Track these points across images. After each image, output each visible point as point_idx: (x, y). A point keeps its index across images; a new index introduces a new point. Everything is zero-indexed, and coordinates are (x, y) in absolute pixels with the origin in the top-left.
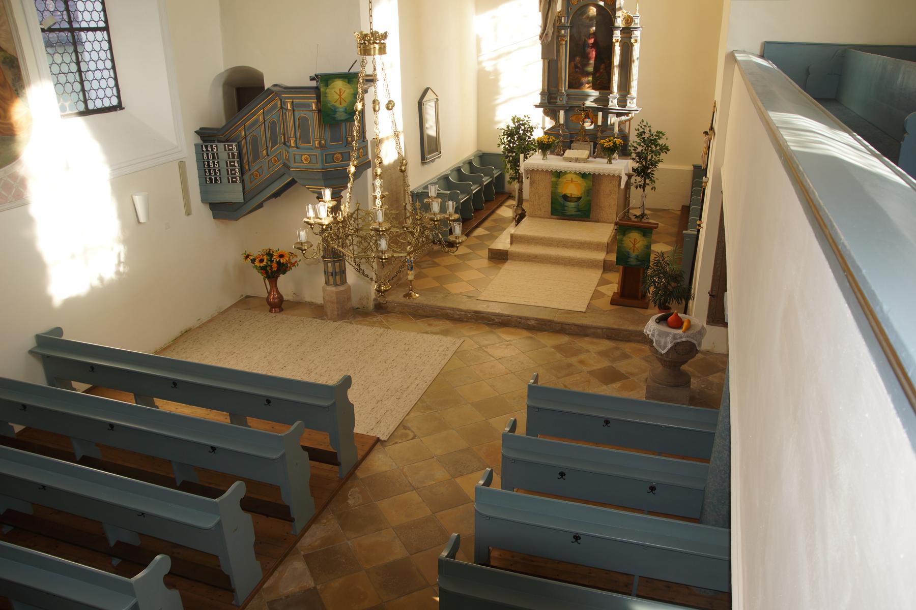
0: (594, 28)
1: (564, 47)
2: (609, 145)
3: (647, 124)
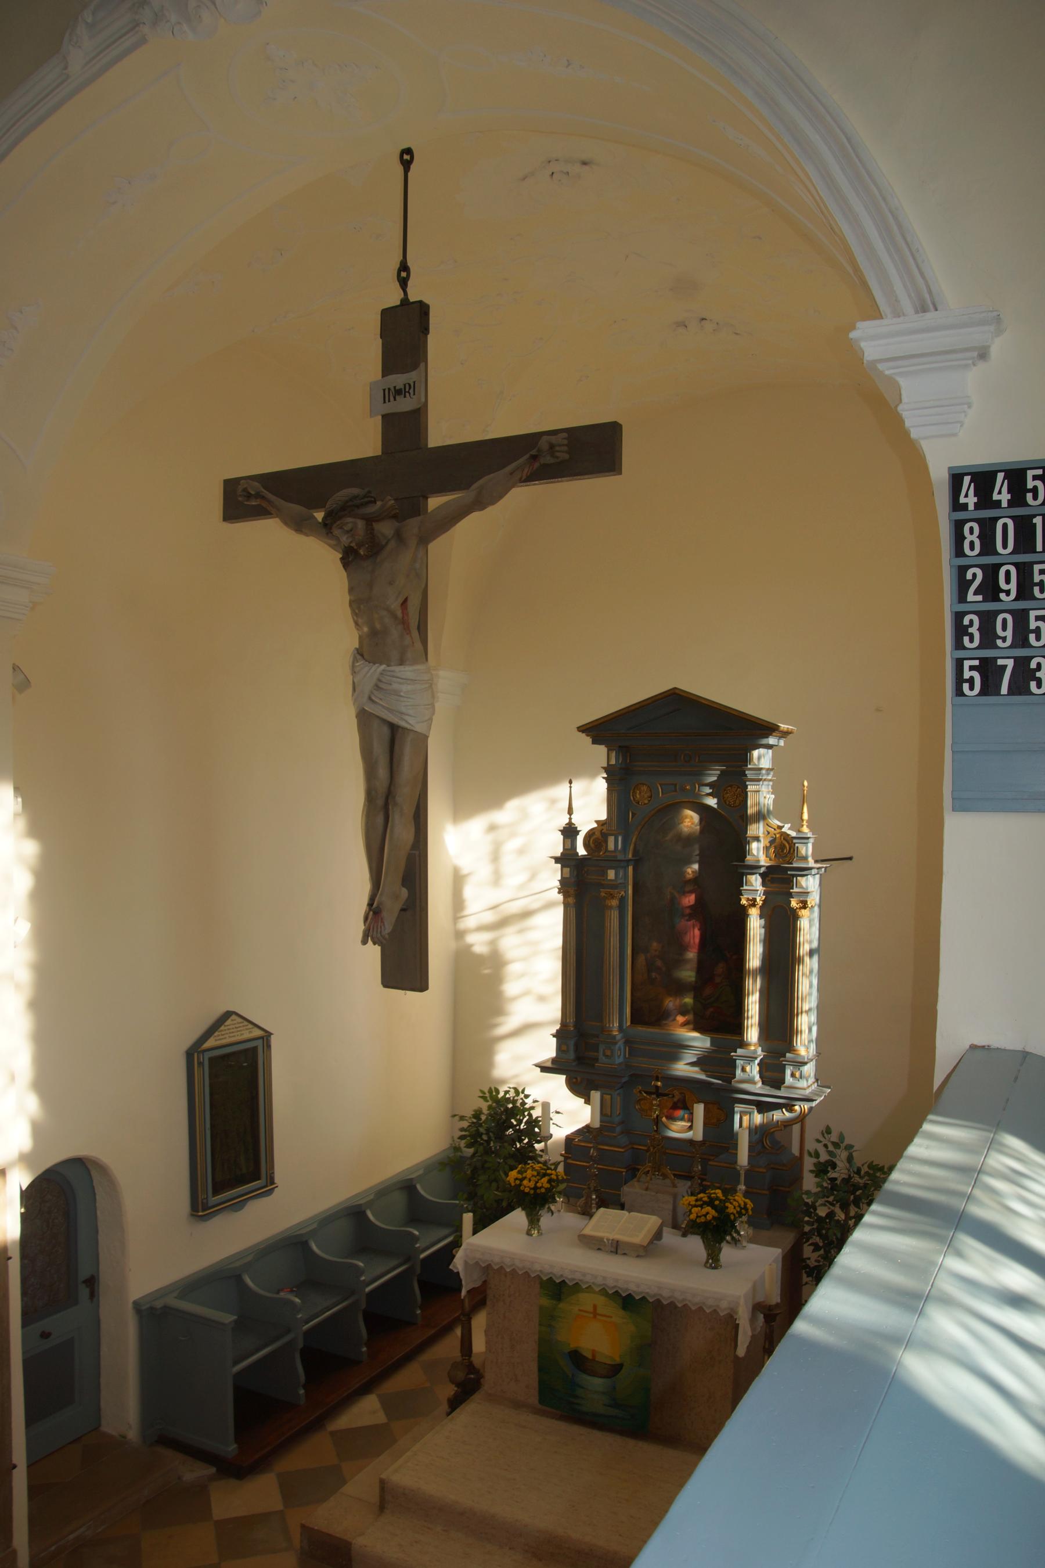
0: (696, 866)
1: (615, 915)
2: (705, 1216)
3: (841, 1137)
